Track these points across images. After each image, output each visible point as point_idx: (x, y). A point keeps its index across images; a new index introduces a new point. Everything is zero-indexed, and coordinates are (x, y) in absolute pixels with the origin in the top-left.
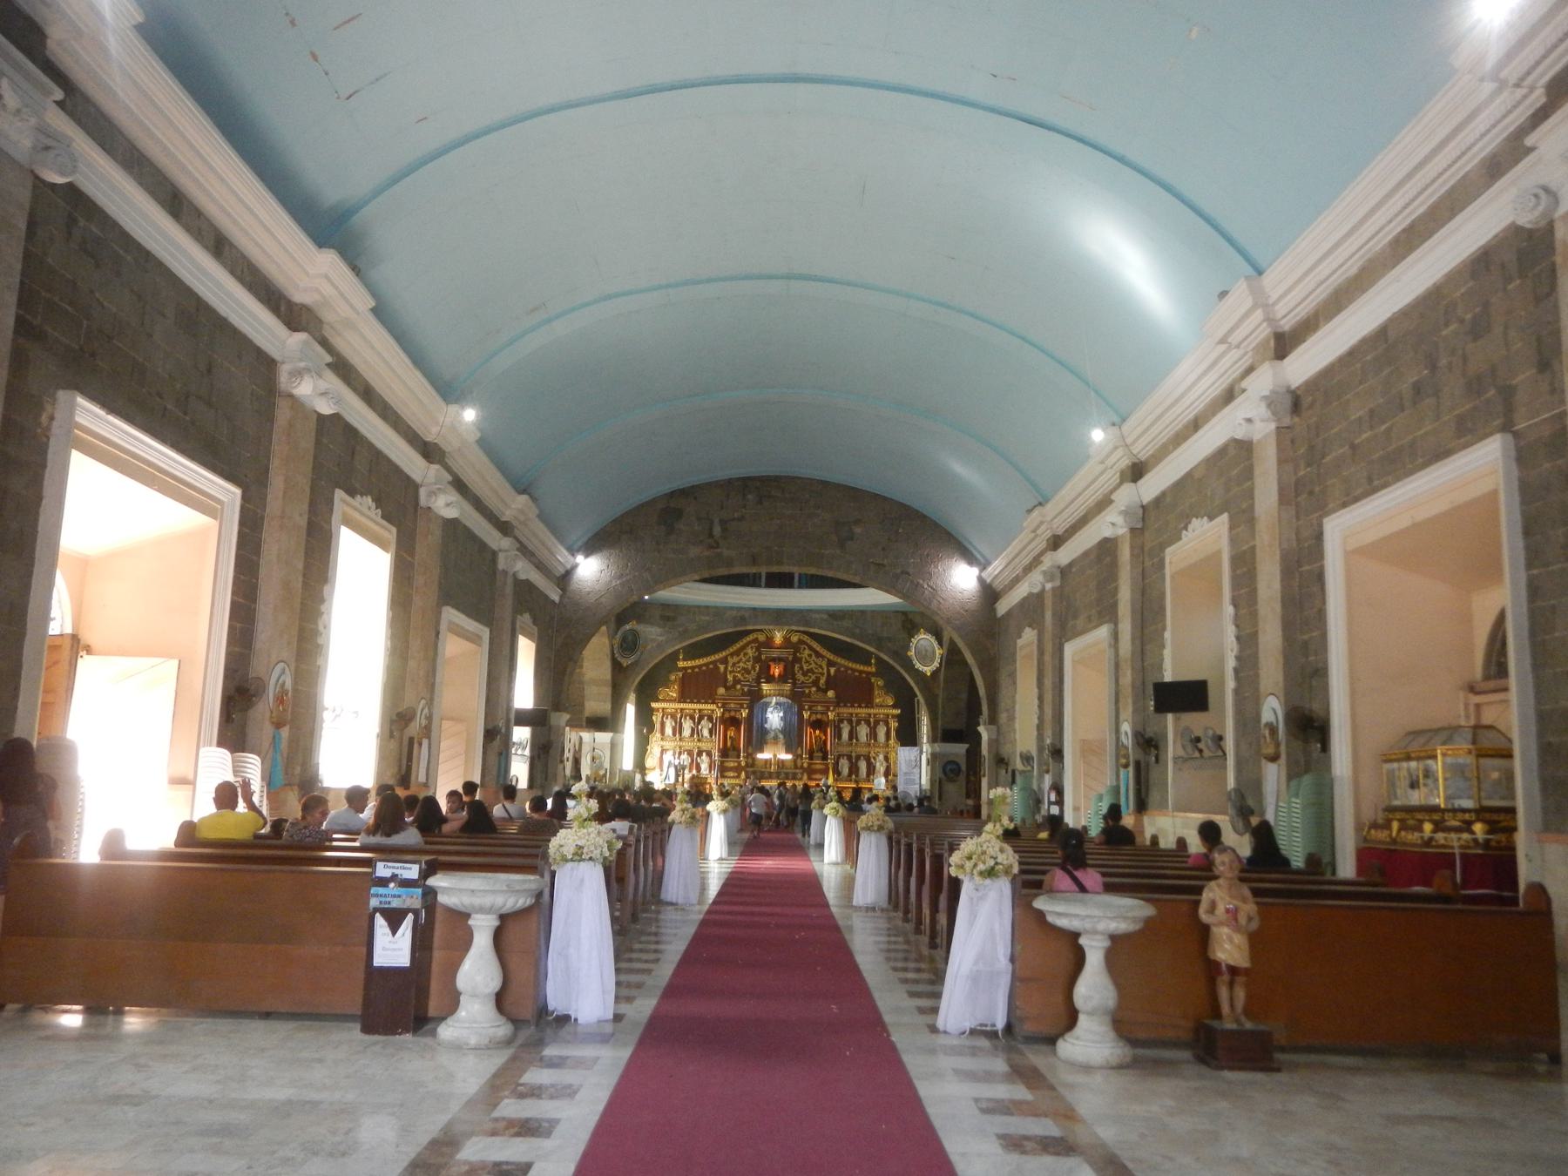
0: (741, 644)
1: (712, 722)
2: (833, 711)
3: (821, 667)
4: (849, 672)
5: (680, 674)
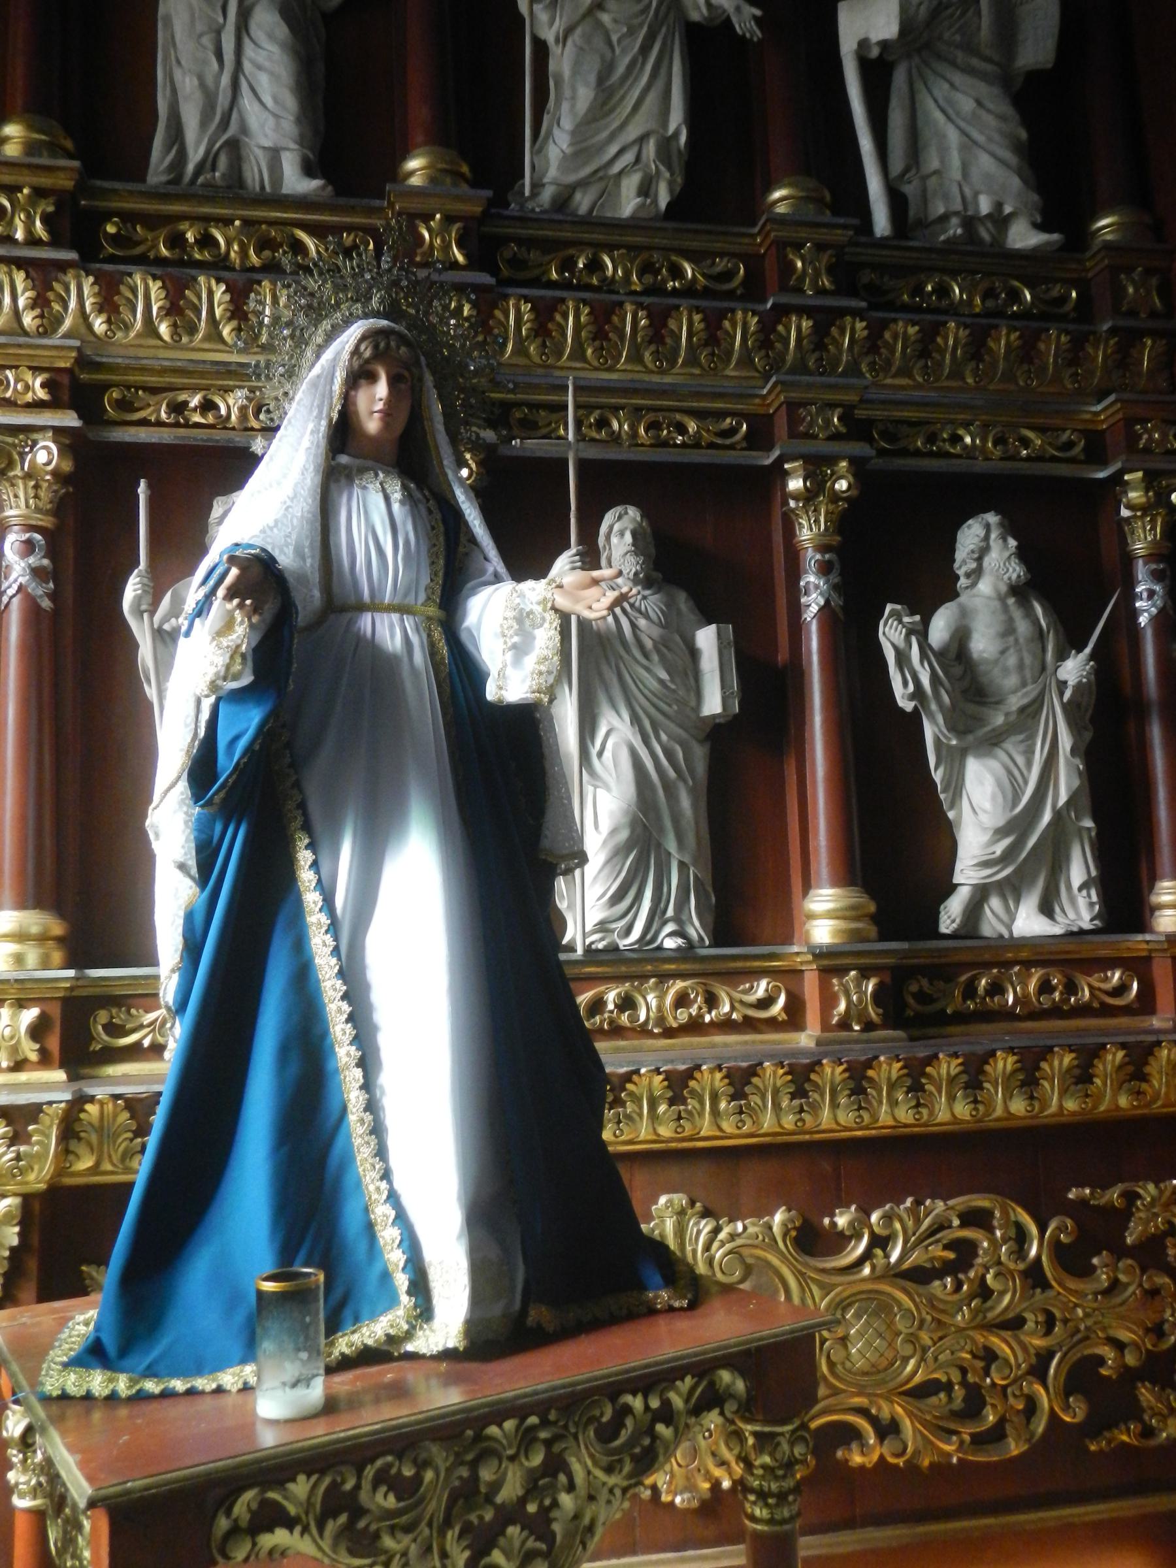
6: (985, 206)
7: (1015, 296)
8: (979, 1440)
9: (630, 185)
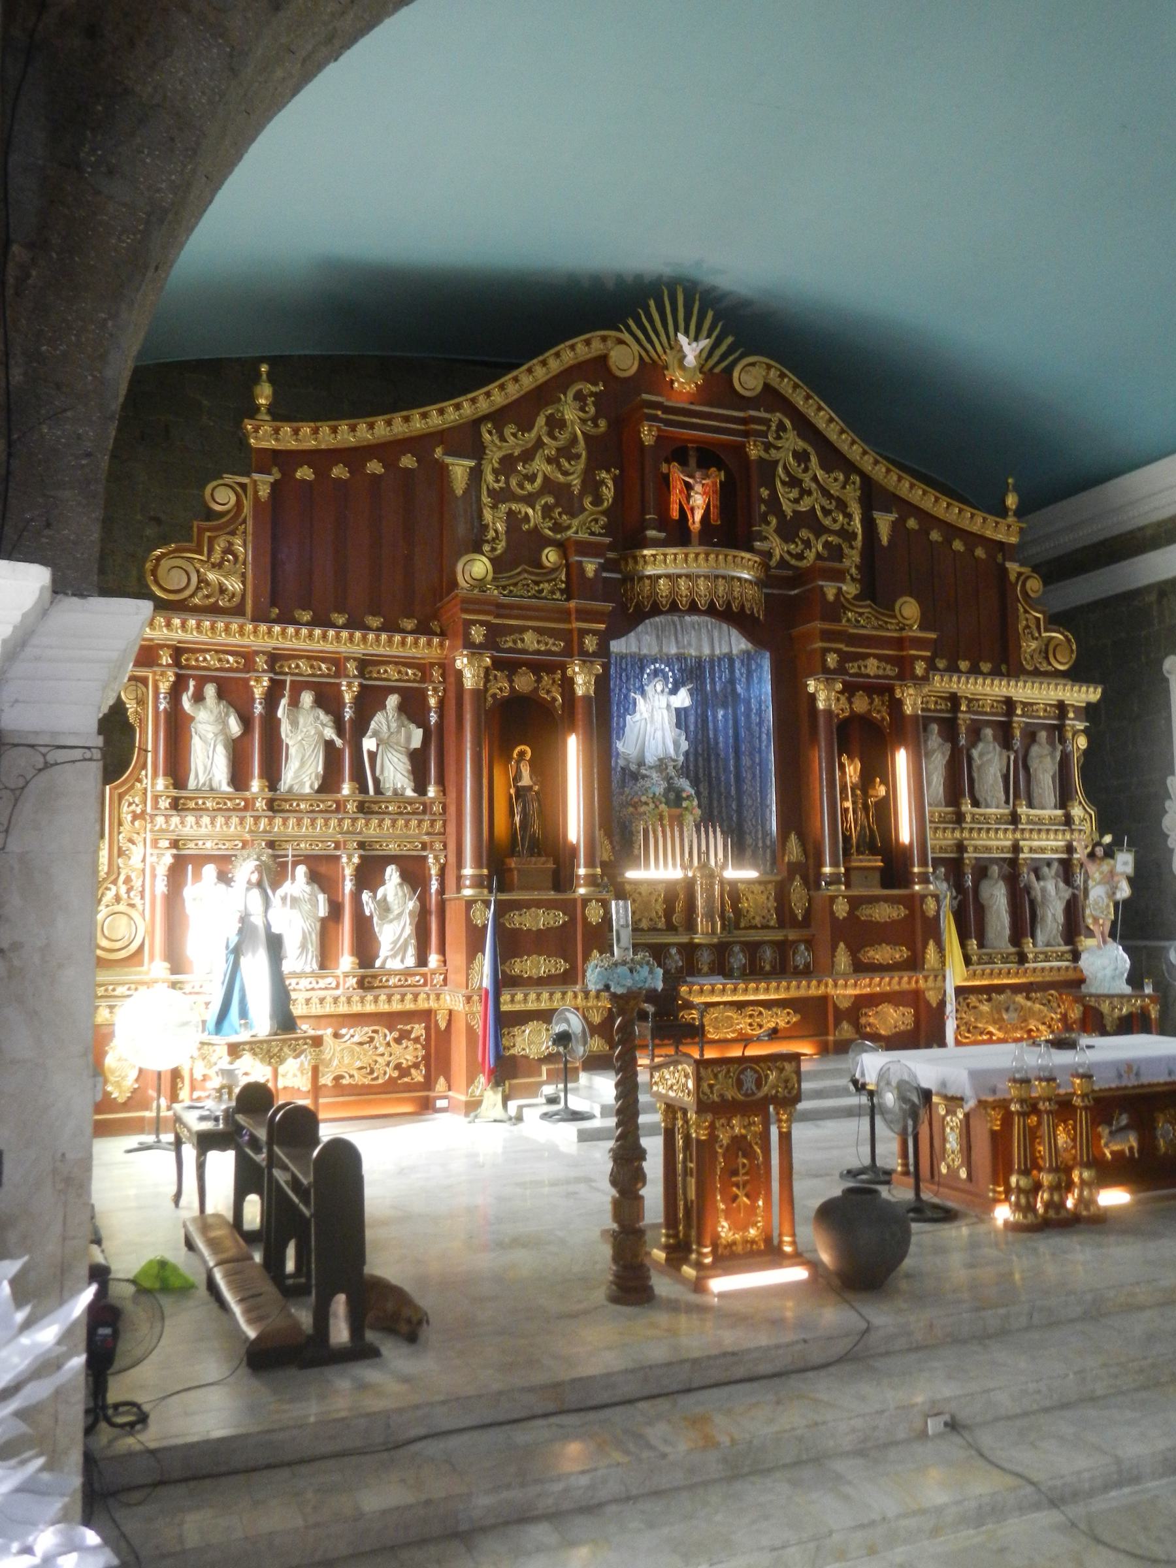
0: (541, 374)
1: (422, 723)
2: (925, 679)
3: (842, 506)
4: (935, 536)
5: (263, 483)
6: (399, 786)
7: (405, 808)
8: (373, 1079)
9: (307, 785)
